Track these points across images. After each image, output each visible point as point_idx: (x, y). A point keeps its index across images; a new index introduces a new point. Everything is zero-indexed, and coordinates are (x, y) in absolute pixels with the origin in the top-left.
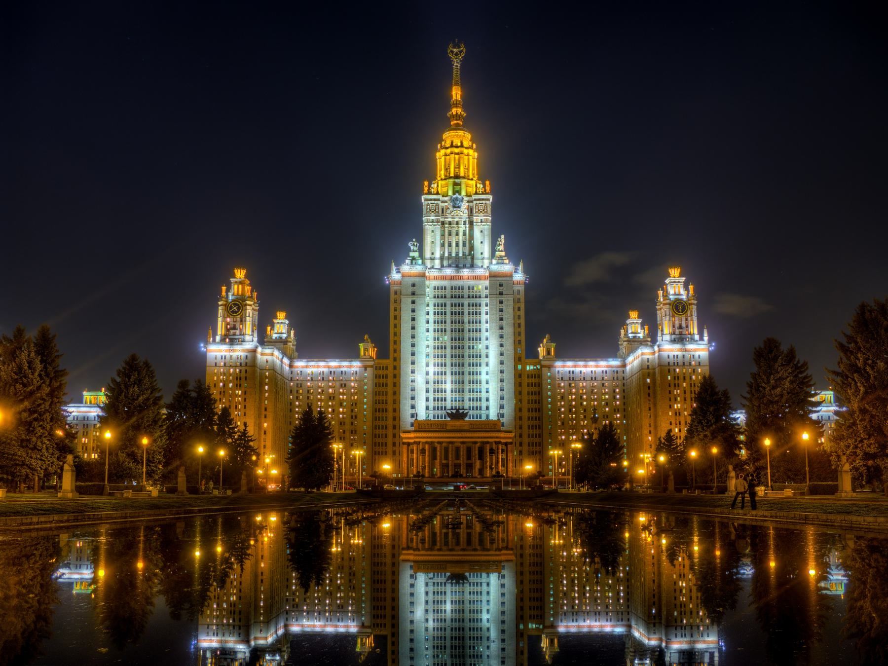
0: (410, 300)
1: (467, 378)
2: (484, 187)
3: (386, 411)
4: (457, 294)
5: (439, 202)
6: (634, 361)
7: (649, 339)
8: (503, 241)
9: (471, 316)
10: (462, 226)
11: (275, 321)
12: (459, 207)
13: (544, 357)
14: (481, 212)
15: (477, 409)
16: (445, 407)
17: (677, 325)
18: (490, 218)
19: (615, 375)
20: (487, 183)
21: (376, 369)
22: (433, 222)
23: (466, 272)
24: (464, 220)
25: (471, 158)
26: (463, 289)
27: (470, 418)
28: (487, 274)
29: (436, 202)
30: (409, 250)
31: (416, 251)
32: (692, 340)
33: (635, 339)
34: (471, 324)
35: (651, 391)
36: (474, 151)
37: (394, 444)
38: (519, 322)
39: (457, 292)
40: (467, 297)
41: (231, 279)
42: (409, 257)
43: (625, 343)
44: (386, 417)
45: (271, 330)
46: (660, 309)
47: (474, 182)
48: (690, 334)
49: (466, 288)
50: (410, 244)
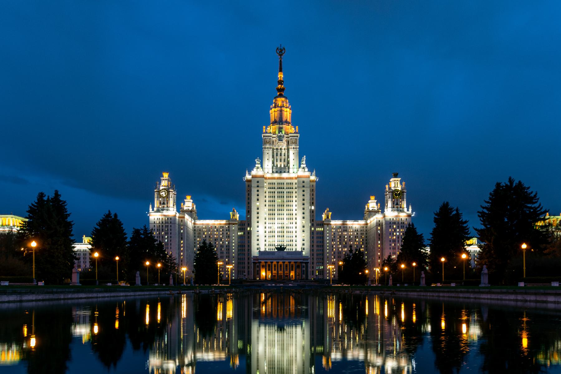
0: (256, 190)
1: (285, 230)
2: (295, 129)
3: (244, 247)
5: (271, 138)
6: (373, 220)
7: (380, 211)
8: (305, 159)
9: (288, 198)
12: (282, 140)
13: (325, 219)
14: (294, 143)
15: (291, 246)
16: (274, 245)
17: (395, 203)
18: (298, 147)
19: (362, 229)
20: (297, 127)
21: (239, 225)
22: (268, 148)
23: (284, 175)
24: (284, 147)
26: (283, 184)
27: (287, 250)
29: (269, 137)
30: (256, 163)
31: (259, 164)
33: (373, 211)
34: (288, 202)
35: (380, 237)
37: (248, 263)
38: (313, 201)
39: (281, 186)
40: (286, 188)
43: (367, 213)
44: (244, 250)
45: (183, 205)
46: (387, 195)
49: (285, 184)
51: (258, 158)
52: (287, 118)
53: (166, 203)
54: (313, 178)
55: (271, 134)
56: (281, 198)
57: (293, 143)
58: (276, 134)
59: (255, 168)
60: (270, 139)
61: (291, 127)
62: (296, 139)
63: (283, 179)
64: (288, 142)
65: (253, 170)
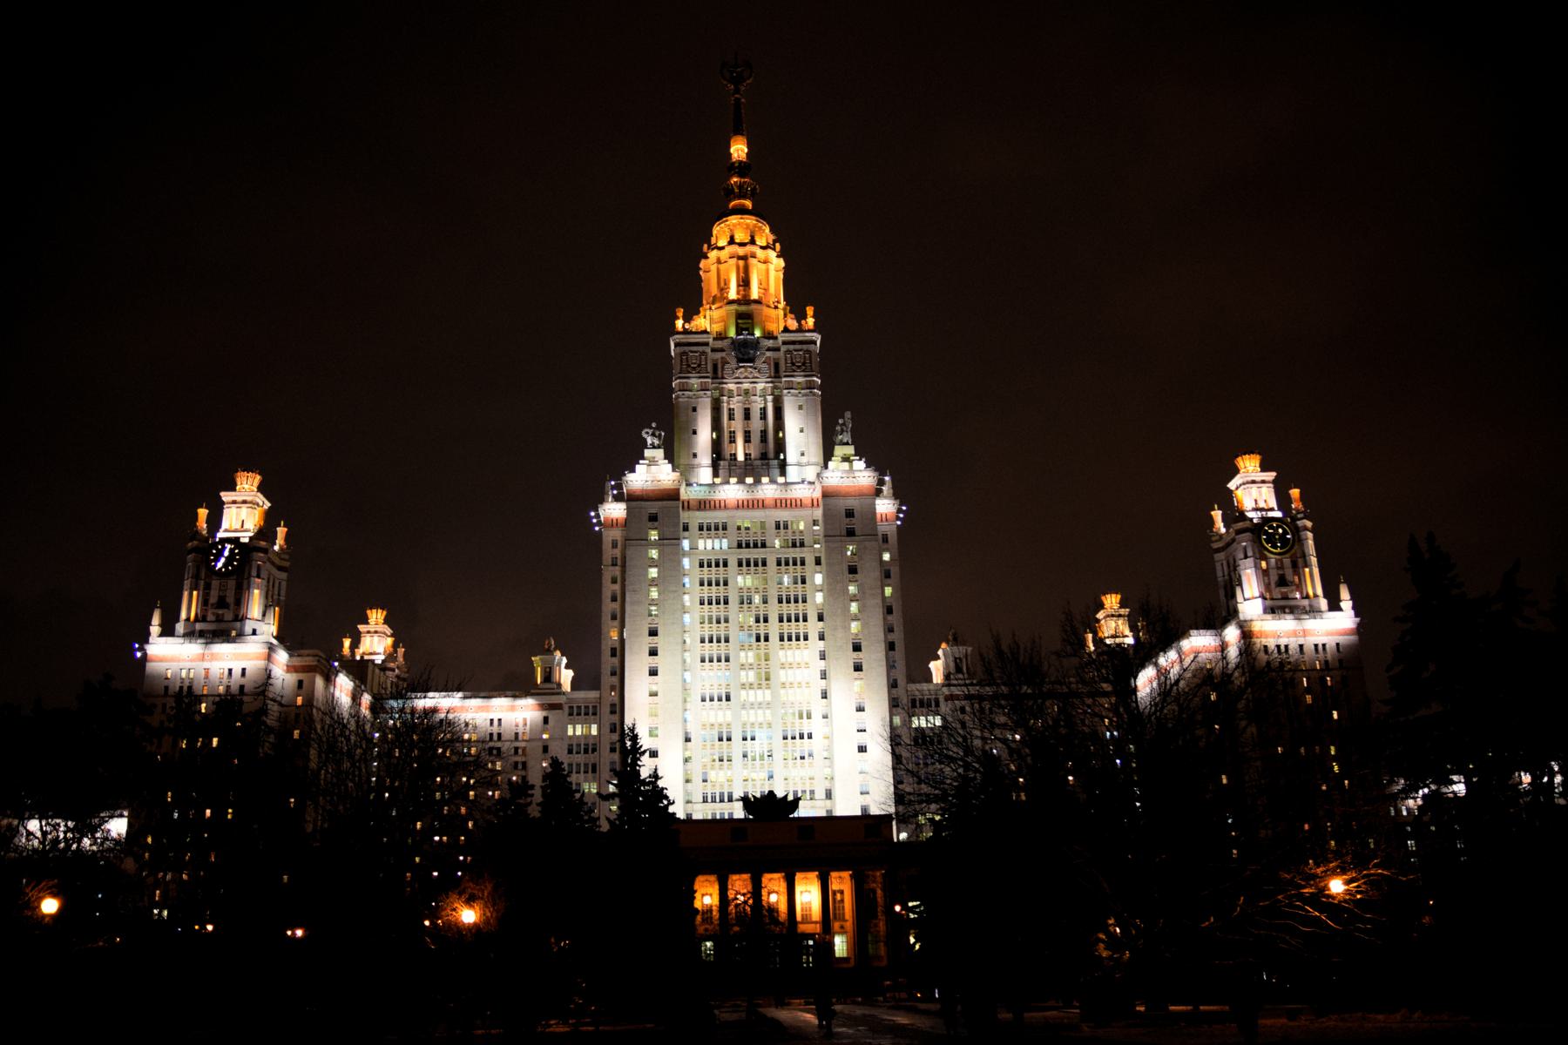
4: (751, 539)
5: (708, 350)
10: (757, 398)
11: (362, 628)
12: (752, 360)
14: (799, 367)
20: (810, 311)
24: (760, 386)
25: (772, 267)
28: (817, 494)
29: (700, 349)
31: (659, 447)
32: (1313, 611)
36: (778, 256)
41: (222, 494)
42: (643, 458)
47: (782, 313)
48: (1307, 597)
50: (645, 436)
51: (654, 425)
52: (768, 284)
53: (230, 599)
54: (885, 506)
55: (705, 336)
56: (752, 568)
57: (794, 367)
58: (726, 338)
59: (641, 462)
60: (703, 353)
61: (785, 316)
62: (808, 352)
63: (759, 504)
64: (777, 366)
65: (633, 471)
